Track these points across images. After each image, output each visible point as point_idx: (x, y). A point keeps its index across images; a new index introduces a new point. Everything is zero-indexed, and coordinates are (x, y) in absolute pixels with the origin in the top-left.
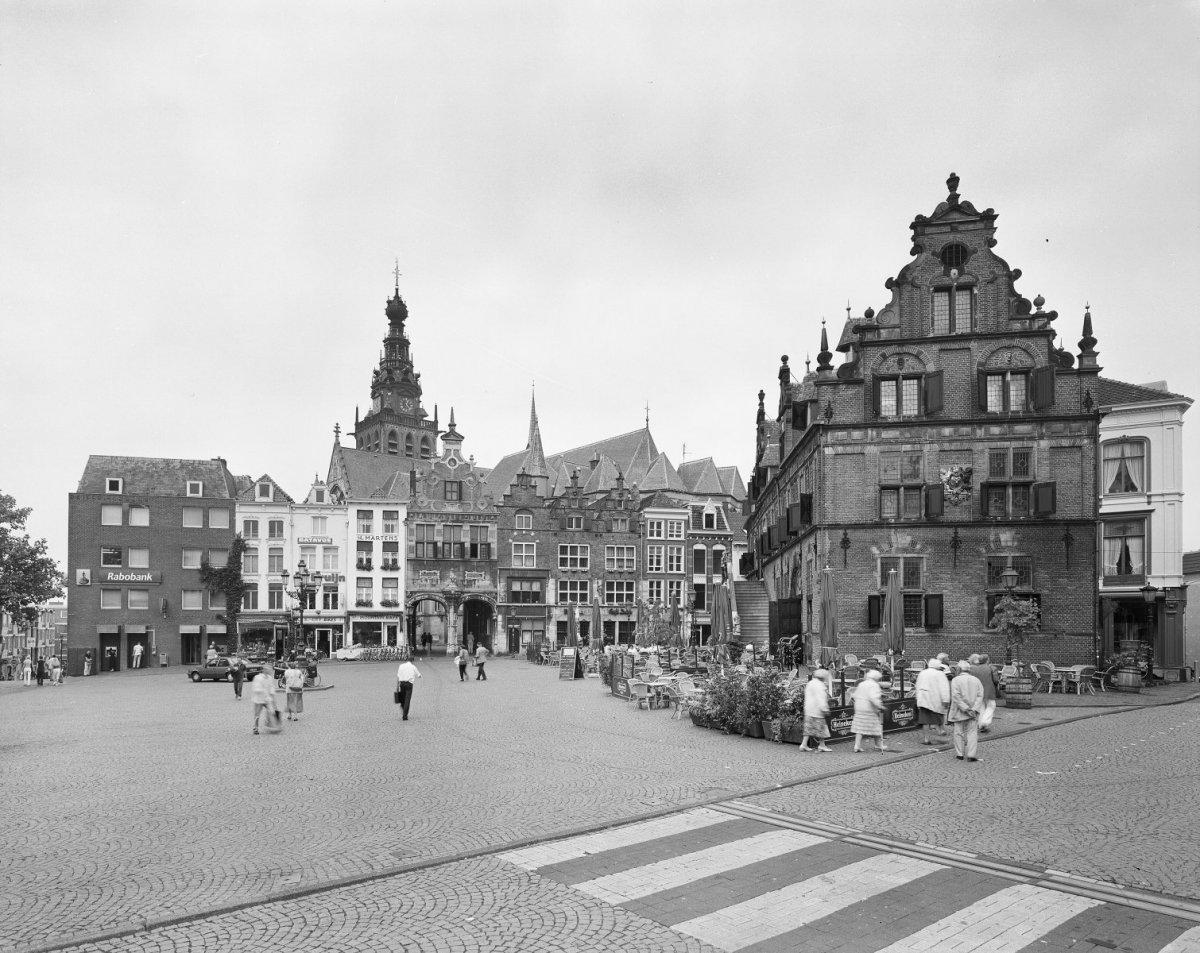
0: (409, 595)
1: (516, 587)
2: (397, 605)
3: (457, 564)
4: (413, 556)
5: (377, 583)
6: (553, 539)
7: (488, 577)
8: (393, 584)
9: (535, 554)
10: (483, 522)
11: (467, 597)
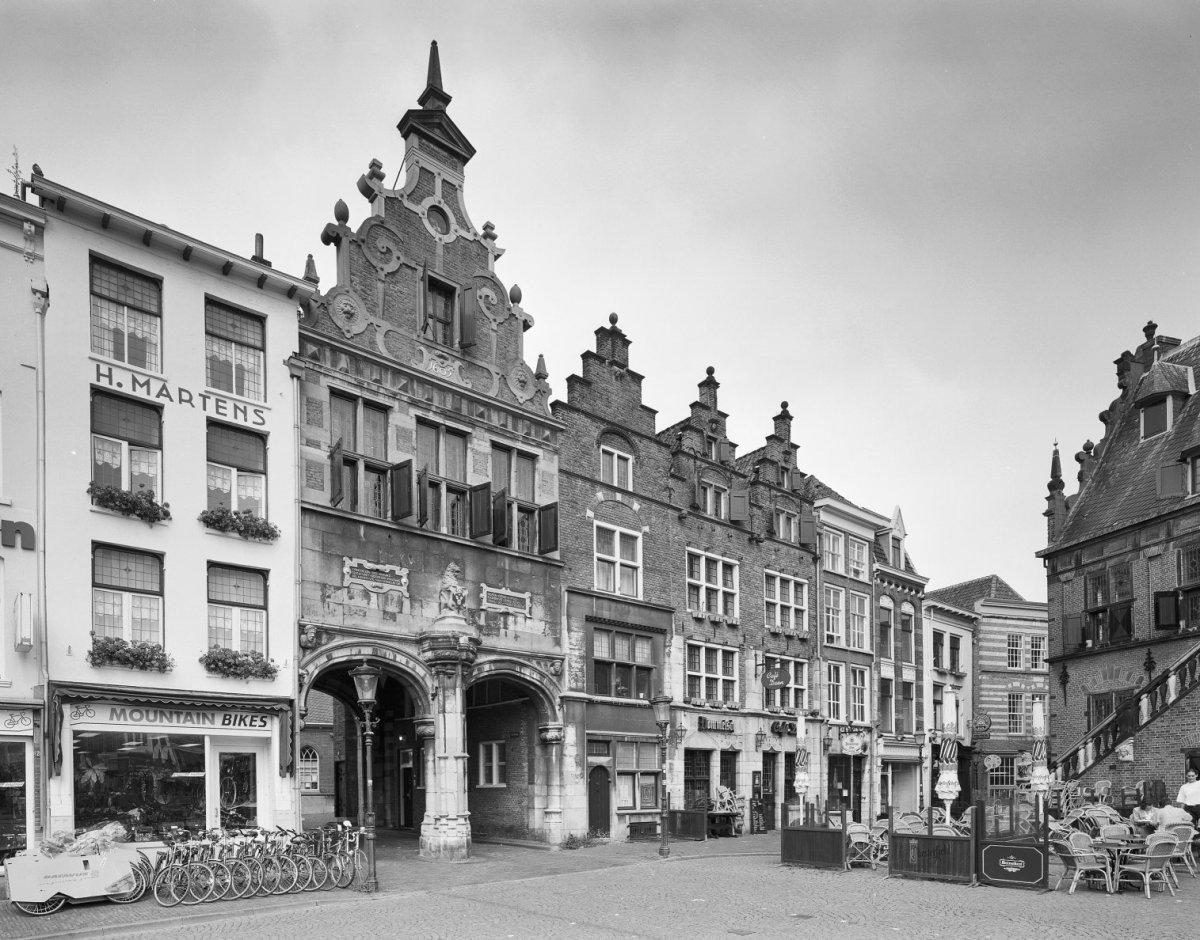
0: (310, 640)
1: (602, 650)
2: (267, 672)
3: (457, 553)
4: (322, 498)
5: (186, 577)
6: (676, 531)
7: (539, 611)
8: (249, 591)
9: (639, 563)
10: (526, 440)
11: (485, 666)
